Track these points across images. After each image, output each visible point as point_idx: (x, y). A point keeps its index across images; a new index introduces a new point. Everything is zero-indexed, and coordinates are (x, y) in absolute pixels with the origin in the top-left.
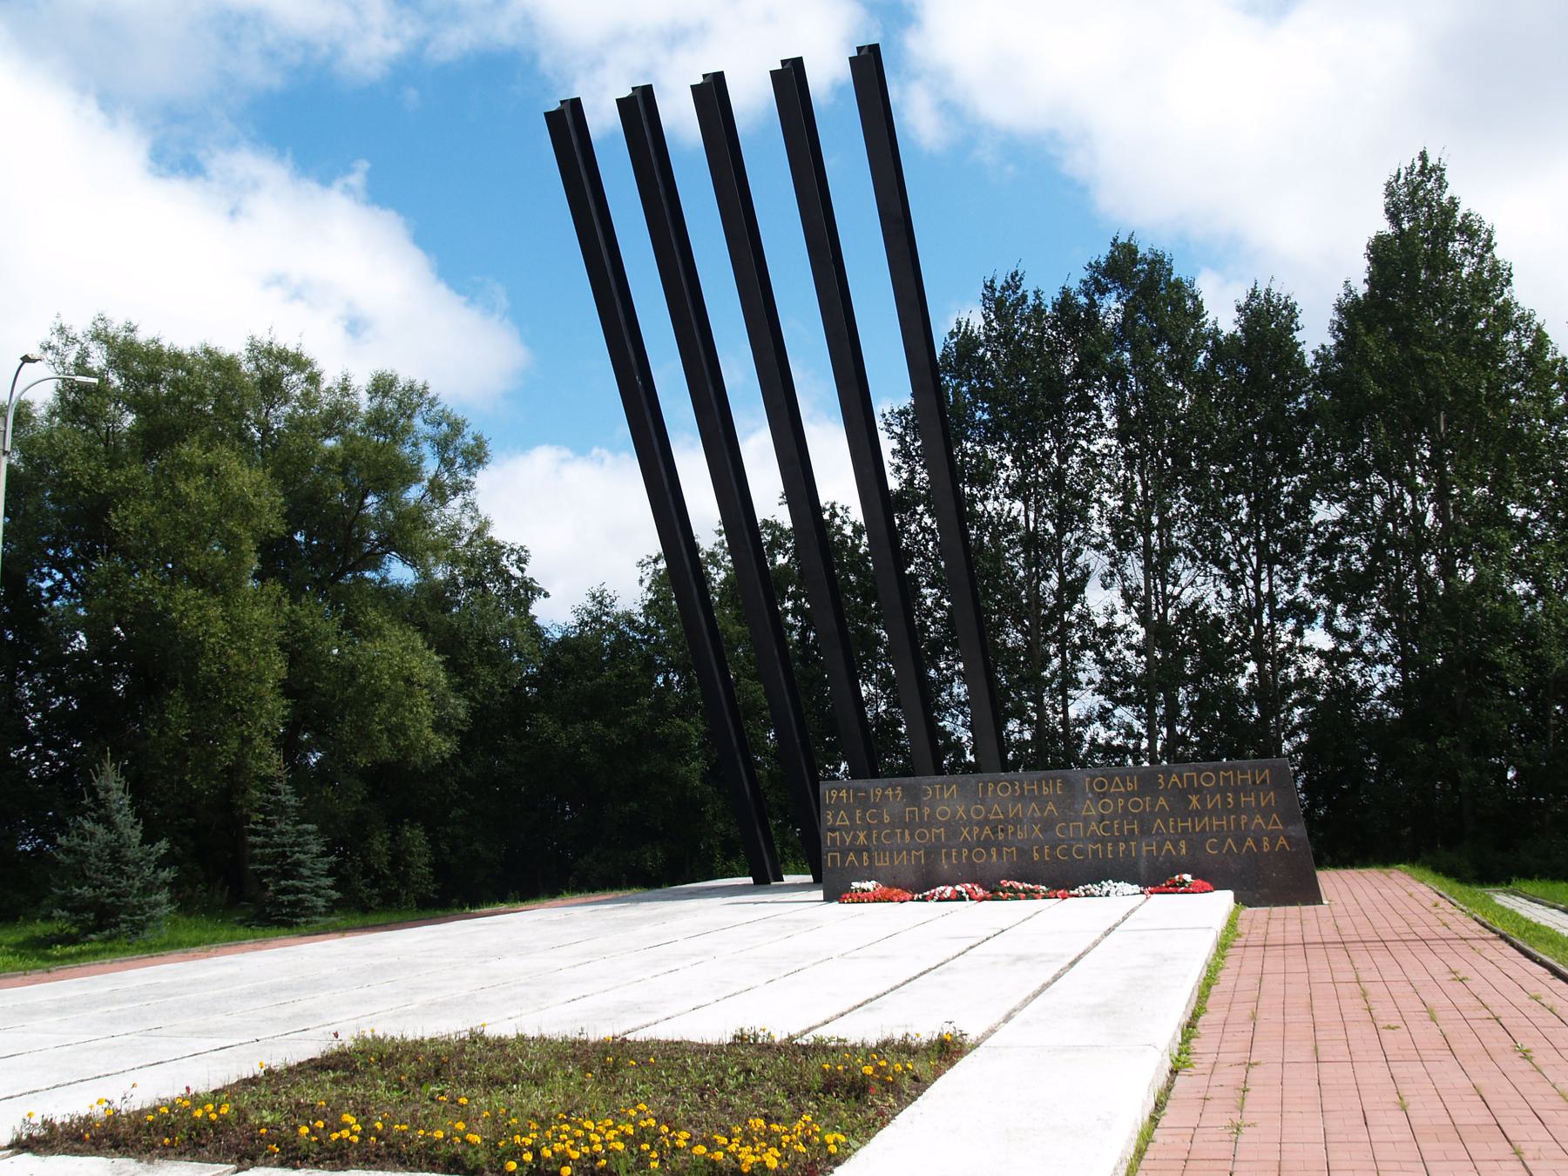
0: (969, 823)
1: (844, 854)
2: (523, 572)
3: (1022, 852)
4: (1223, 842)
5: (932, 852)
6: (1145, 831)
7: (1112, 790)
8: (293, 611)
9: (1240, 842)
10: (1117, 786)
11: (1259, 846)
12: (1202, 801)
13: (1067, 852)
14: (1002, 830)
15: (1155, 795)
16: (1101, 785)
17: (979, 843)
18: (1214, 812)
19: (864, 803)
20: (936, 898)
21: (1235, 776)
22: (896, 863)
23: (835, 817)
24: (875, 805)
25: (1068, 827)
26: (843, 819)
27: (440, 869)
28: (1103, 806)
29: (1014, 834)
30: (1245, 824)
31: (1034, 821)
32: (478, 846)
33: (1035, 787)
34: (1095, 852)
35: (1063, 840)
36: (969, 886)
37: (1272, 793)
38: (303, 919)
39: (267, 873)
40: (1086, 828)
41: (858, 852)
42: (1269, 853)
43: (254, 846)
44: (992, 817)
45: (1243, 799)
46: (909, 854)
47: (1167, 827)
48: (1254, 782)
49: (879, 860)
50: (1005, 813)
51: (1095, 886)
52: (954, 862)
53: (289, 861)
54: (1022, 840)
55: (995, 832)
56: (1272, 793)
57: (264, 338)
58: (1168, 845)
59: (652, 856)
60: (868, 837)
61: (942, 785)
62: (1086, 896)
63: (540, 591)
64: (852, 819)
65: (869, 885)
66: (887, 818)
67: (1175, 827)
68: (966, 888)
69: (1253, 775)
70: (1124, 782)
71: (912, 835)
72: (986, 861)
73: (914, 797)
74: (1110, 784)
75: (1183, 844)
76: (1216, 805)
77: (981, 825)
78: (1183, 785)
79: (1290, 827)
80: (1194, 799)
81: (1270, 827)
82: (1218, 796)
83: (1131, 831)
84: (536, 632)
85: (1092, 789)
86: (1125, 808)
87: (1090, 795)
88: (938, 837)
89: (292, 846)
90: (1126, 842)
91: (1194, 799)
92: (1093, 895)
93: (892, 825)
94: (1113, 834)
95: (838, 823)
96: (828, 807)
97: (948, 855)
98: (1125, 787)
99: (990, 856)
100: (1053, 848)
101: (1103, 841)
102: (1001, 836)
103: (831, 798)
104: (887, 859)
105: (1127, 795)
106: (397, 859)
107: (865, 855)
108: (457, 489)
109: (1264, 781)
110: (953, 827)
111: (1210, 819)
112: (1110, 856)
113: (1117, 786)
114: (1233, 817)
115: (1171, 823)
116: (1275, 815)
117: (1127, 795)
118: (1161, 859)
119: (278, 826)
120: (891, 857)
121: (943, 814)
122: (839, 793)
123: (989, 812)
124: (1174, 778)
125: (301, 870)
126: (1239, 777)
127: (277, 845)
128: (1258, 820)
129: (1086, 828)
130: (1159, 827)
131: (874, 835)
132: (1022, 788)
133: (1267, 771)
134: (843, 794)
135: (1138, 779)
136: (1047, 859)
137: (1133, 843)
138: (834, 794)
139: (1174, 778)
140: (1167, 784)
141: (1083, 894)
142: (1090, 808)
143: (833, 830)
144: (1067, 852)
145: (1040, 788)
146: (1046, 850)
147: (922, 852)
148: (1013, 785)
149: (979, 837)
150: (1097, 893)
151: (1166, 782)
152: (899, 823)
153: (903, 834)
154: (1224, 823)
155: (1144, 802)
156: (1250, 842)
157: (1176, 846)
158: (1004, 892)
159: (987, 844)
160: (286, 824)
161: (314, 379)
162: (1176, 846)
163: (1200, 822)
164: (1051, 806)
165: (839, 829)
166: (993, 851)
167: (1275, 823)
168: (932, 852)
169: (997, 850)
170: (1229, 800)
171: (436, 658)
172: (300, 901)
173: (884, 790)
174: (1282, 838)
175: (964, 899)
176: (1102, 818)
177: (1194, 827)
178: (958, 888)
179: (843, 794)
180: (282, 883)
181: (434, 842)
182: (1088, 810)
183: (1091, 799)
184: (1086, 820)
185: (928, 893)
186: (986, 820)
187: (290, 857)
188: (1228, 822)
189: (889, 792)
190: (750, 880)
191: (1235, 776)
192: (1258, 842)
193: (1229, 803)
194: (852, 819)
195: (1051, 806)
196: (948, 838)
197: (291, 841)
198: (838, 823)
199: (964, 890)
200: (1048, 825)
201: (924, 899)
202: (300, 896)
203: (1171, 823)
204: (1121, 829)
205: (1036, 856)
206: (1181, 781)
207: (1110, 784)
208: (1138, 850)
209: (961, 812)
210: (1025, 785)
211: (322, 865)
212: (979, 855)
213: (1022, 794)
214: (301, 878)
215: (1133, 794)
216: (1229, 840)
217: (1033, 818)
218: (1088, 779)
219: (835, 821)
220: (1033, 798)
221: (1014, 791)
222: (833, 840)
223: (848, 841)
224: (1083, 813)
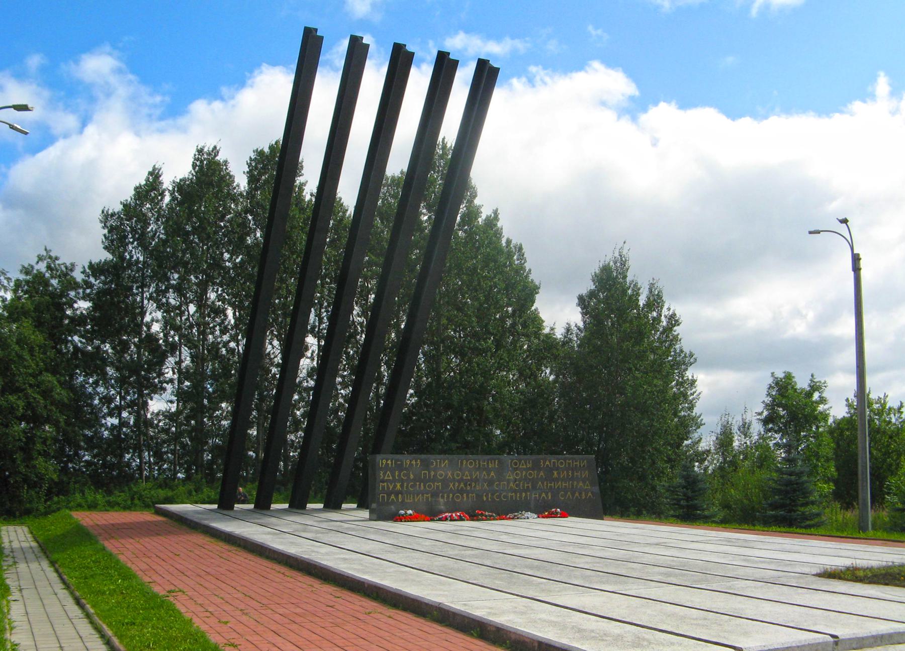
0: (454, 480)
1: (389, 495)
3: (479, 497)
6: (534, 487)
9: (573, 496)
11: (581, 497)
12: (559, 474)
13: (499, 497)
16: (516, 464)
19: (400, 468)
20: (449, 519)
21: (573, 463)
23: (384, 474)
24: (406, 469)
25: (500, 484)
26: (388, 476)
29: (475, 487)
31: (485, 480)
34: (512, 497)
35: (497, 491)
41: (397, 494)
44: (465, 478)
48: (580, 466)
50: (471, 475)
55: (466, 486)
56: (587, 472)
58: (544, 495)
60: (402, 486)
64: (394, 476)
65: (410, 512)
66: (412, 476)
67: (547, 486)
69: (580, 463)
70: (526, 463)
73: (426, 465)
74: (520, 464)
75: (550, 495)
77: (459, 481)
80: (555, 473)
81: (586, 487)
85: (511, 466)
86: (526, 475)
88: (438, 487)
91: (555, 473)
93: (414, 480)
94: (520, 488)
95: (386, 478)
96: (381, 469)
99: (464, 498)
100: (493, 495)
101: (515, 491)
102: (469, 488)
103: (382, 464)
104: (411, 498)
105: (527, 469)
107: (400, 495)
109: (584, 466)
110: (445, 482)
117: (527, 469)
120: (414, 498)
121: (441, 475)
122: (387, 461)
124: (547, 463)
128: (581, 484)
130: (540, 486)
131: (405, 485)
132: (479, 464)
135: (532, 462)
139: (547, 463)
142: (510, 476)
143: (383, 481)
144: (499, 497)
145: (488, 464)
146: (490, 496)
149: (458, 489)
151: (544, 463)
152: (418, 479)
153: (420, 485)
156: (577, 494)
157: (547, 495)
159: (461, 491)
162: (547, 495)
165: (387, 481)
166: (465, 495)
175: (463, 520)
176: (516, 480)
177: (554, 486)
179: (389, 462)
184: (508, 481)
186: (462, 479)
188: (569, 484)
189: (414, 462)
191: (573, 463)
192: (580, 494)
194: (394, 476)
195: (492, 474)
198: (386, 478)
200: (491, 483)
204: (523, 486)
205: (485, 499)
206: (550, 464)
207: (520, 464)
209: (450, 474)
210: (481, 463)
213: (479, 466)
215: (529, 469)
218: (510, 461)
219: (384, 477)
222: (383, 487)
223: (391, 488)
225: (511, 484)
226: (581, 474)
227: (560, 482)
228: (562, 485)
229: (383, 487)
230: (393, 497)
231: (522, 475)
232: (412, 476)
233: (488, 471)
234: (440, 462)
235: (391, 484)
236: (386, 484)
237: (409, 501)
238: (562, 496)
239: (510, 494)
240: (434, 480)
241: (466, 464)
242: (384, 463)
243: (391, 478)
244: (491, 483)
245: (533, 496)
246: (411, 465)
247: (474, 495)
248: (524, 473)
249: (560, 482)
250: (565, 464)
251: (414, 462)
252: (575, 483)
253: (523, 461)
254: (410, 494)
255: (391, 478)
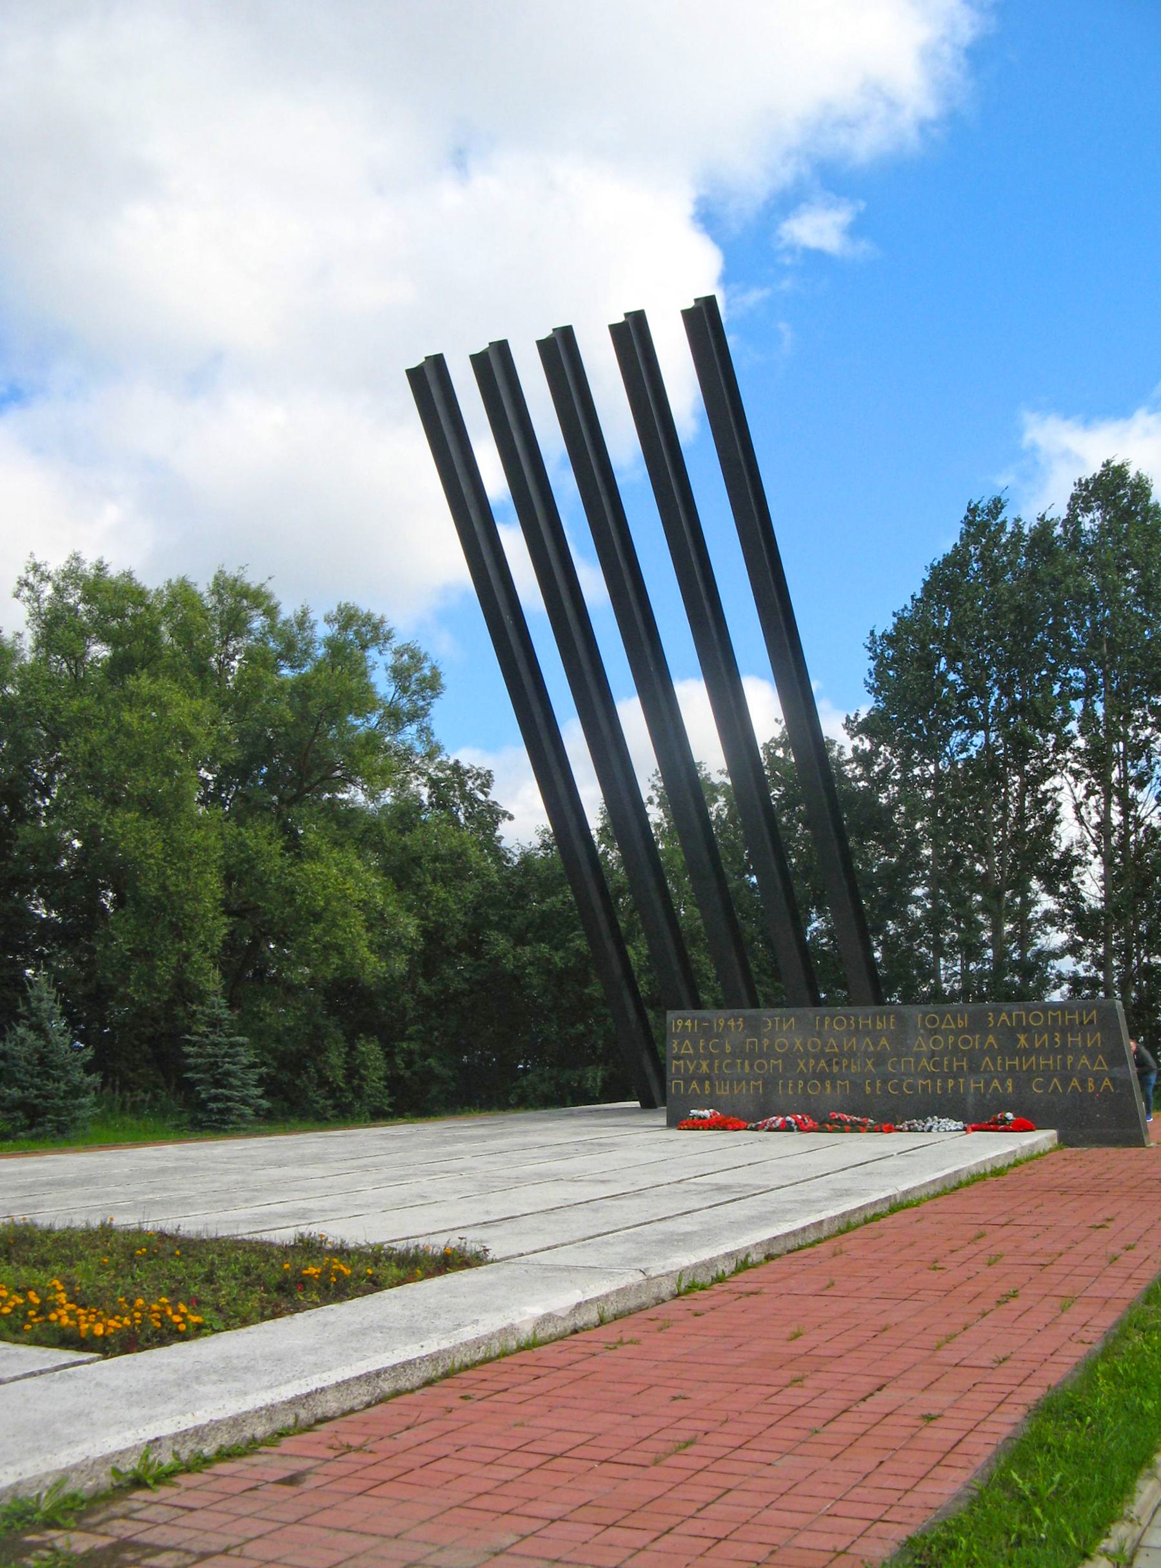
1: (688, 1081)
2: (486, 796)
3: (856, 1086)
4: (1049, 1081)
5: (769, 1082)
6: (974, 1069)
7: (943, 1027)
8: (240, 834)
9: (1065, 1081)
10: (948, 1023)
12: (1030, 1040)
13: (897, 1087)
14: (837, 1063)
15: (985, 1031)
16: (933, 1022)
17: (815, 1075)
18: (1040, 1051)
19: (707, 1032)
20: (767, 1127)
21: (1063, 1016)
22: (736, 1092)
23: (680, 1044)
24: (718, 1036)
25: (900, 1061)
26: (687, 1048)
27: (394, 1083)
28: (935, 1042)
29: (848, 1067)
30: (1071, 1064)
31: (867, 1055)
32: (432, 1061)
33: (870, 1021)
35: (894, 1074)
36: (799, 1117)
37: (1099, 1034)
38: (231, 1126)
39: (201, 1081)
40: (917, 1062)
41: (701, 1080)
42: (1093, 1093)
43: (188, 1056)
44: (827, 1050)
45: (1070, 1039)
46: (748, 1084)
47: (995, 1065)
48: (1081, 1023)
49: (720, 1089)
50: (840, 1046)
51: (920, 1121)
52: (790, 1093)
53: (220, 1070)
54: (855, 1074)
56: (1099, 1034)
57: (232, 571)
58: (996, 1083)
59: (595, 1076)
60: (710, 1066)
61: (781, 1017)
62: (910, 1131)
63: (505, 814)
65: (706, 1113)
66: (728, 1048)
67: (1003, 1065)
68: (796, 1119)
69: (1081, 1015)
70: (955, 1019)
71: (751, 1066)
72: (821, 1091)
73: (754, 1028)
75: (1009, 1083)
76: (1043, 1045)
78: (1011, 1023)
79: (1115, 1069)
80: (1022, 1038)
82: (1046, 1036)
83: (961, 1068)
84: (499, 855)
85: (924, 1026)
86: (955, 1044)
87: (922, 1031)
88: (776, 1067)
89: (224, 1056)
90: (955, 1078)
92: (916, 1130)
93: (733, 1055)
95: (682, 1052)
96: (674, 1036)
97: (785, 1086)
98: (956, 1023)
100: (884, 1082)
101: (932, 1077)
102: (835, 1069)
104: (728, 1088)
106: (352, 1072)
107: (707, 1082)
108: (413, 716)
109: (1091, 1022)
110: (790, 1058)
111: (1037, 1059)
112: (939, 1092)
113: (948, 1023)
114: (1059, 1057)
115: (999, 1062)
116: (1100, 1057)
117: (958, 1033)
118: (988, 1096)
119: (211, 1037)
120: (731, 1086)
121: (782, 1046)
122: (684, 1022)
123: (825, 1044)
124: (1004, 1017)
125: (231, 1080)
126: (1067, 1017)
127: (210, 1056)
128: (1084, 1060)
129: (917, 1062)
131: (716, 1064)
132: (857, 1022)
133: (1094, 1012)
134: (688, 1023)
135: (969, 1016)
136: (879, 1093)
137: (961, 1080)
138: (680, 1023)
139: (1004, 1017)
140: (996, 1024)
141: (907, 1128)
142: (923, 1045)
143: (678, 1058)
145: (874, 1022)
146: (878, 1085)
147: (760, 1082)
148: (848, 1019)
149: (814, 1072)
150: (920, 1128)
153: (743, 1063)
154: (1051, 1062)
155: (974, 1040)
156: (1075, 1082)
157: (1002, 1084)
158: (830, 1124)
159: (822, 1076)
160: (220, 1036)
161: (271, 612)
163: (1027, 1061)
164: (884, 1041)
167: (1101, 1064)
168: (769, 1082)
169: (832, 1083)
170: (1057, 1039)
171: (374, 880)
172: (229, 1110)
173: (726, 1020)
174: (1107, 1079)
175: (791, 1130)
178: (789, 1118)
179: (688, 1023)
180: (213, 1091)
181: (389, 1055)
182: (920, 1046)
183: (922, 1035)
184: (918, 1056)
185: (760, 1123)
186: (822, 1051)
187: (222, 1067)
188: (1055, 1061)
189: (732, 1023)
190: (637, 1104)
191: (1063, 1016)
192: (1083, 1083)
193: (1057, 1043)
194: (696, 1048)
195: (884, 1041)
196: (784, 1068)
197: (222, 1052)
198: (682, 1052)
199: (793, 1121)
200: (880, 1059)
201: (755, 1129)
202: (229, 1104)
203: (999, 1062)
204: (950, 1066)
205: (868, 1090)
207: (942, 1022)
208: (966, 1086)
211: (252, 1076)
212: (814, 1087)
214: (232, 1087)
215: (963, 1031)
216: (1055, 1080)
217: (866, 1052)
218: (920, 1015)
219: (680, 1049)
220: (868, 1033)
221: (849, 1024)
222: (678, 1068)
223: (691, 1068)
224: (915, 1049)
225: (924, 1061)
226: (1084, 1040)
227: (1034, 1058)
228: (1038, 1065)
229: (678, 1068)
230: (694, 1085)
231: (946, 1041)
232: (728, 1048)
233: (875, 1036)
234: (781, 1021)
235: (692, 1062)
236: (682, 1062)
237: (723, 1093)
238: (1038, 1087)
239: (921, 1081)
240: (769, 1055)
241: (831, 1025)
242: (680, 1025)
243: (691, 1051)
244: (880, 1059)
245: (972, 1086)
246: (727, 1027)
247: (847, 1082)
248: (951, 1039)
249: (1034, 1058)
250: (1046, 1021)
251: (732, 1023)
252: (1070, 1059)
253: (949, 1016)
254: (725, 1081)
255: (691, 1051)
